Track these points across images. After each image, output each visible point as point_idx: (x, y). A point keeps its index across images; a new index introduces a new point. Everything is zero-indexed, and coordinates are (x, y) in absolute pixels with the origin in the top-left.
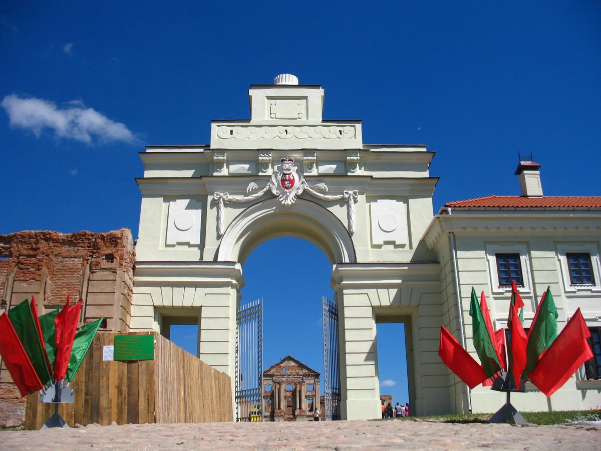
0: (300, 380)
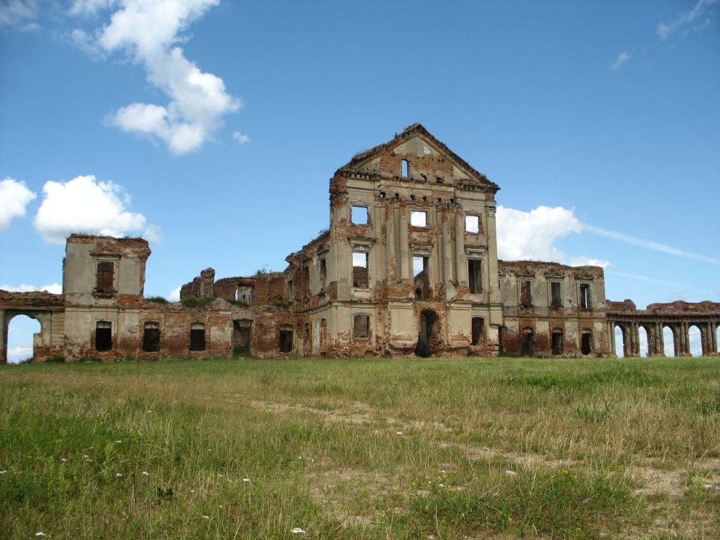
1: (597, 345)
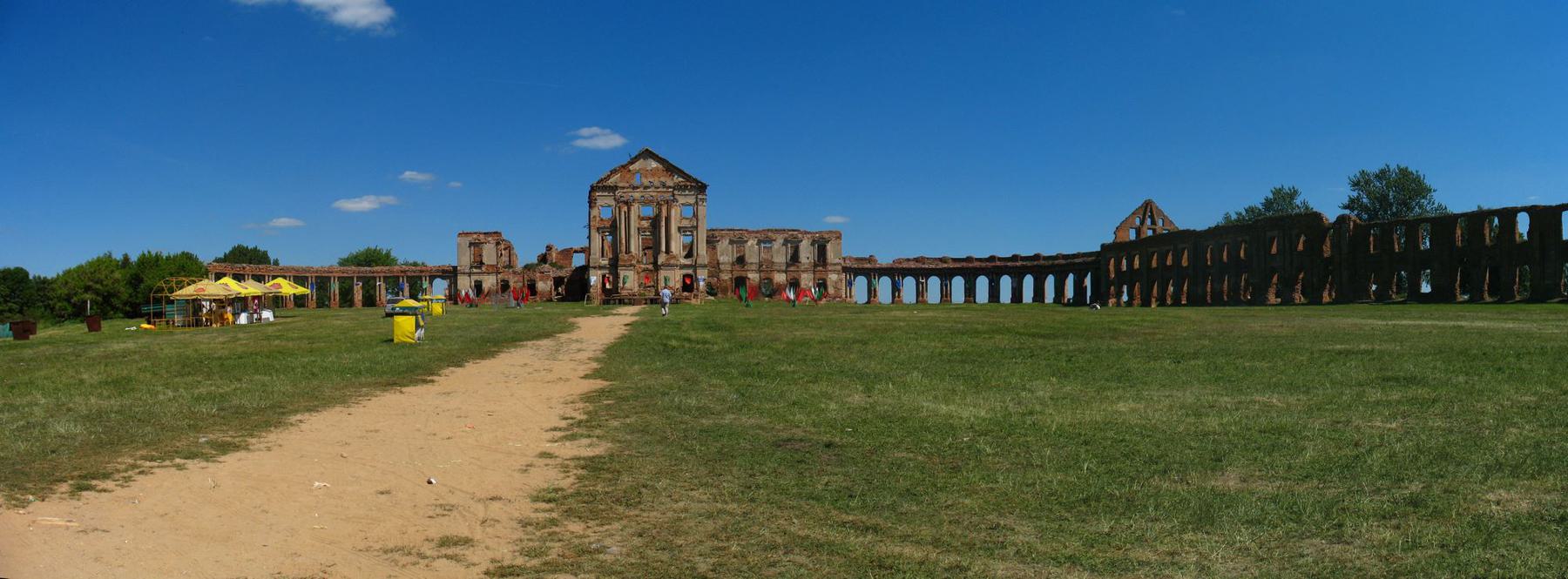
0: (668, 196)
1: (831, 290)
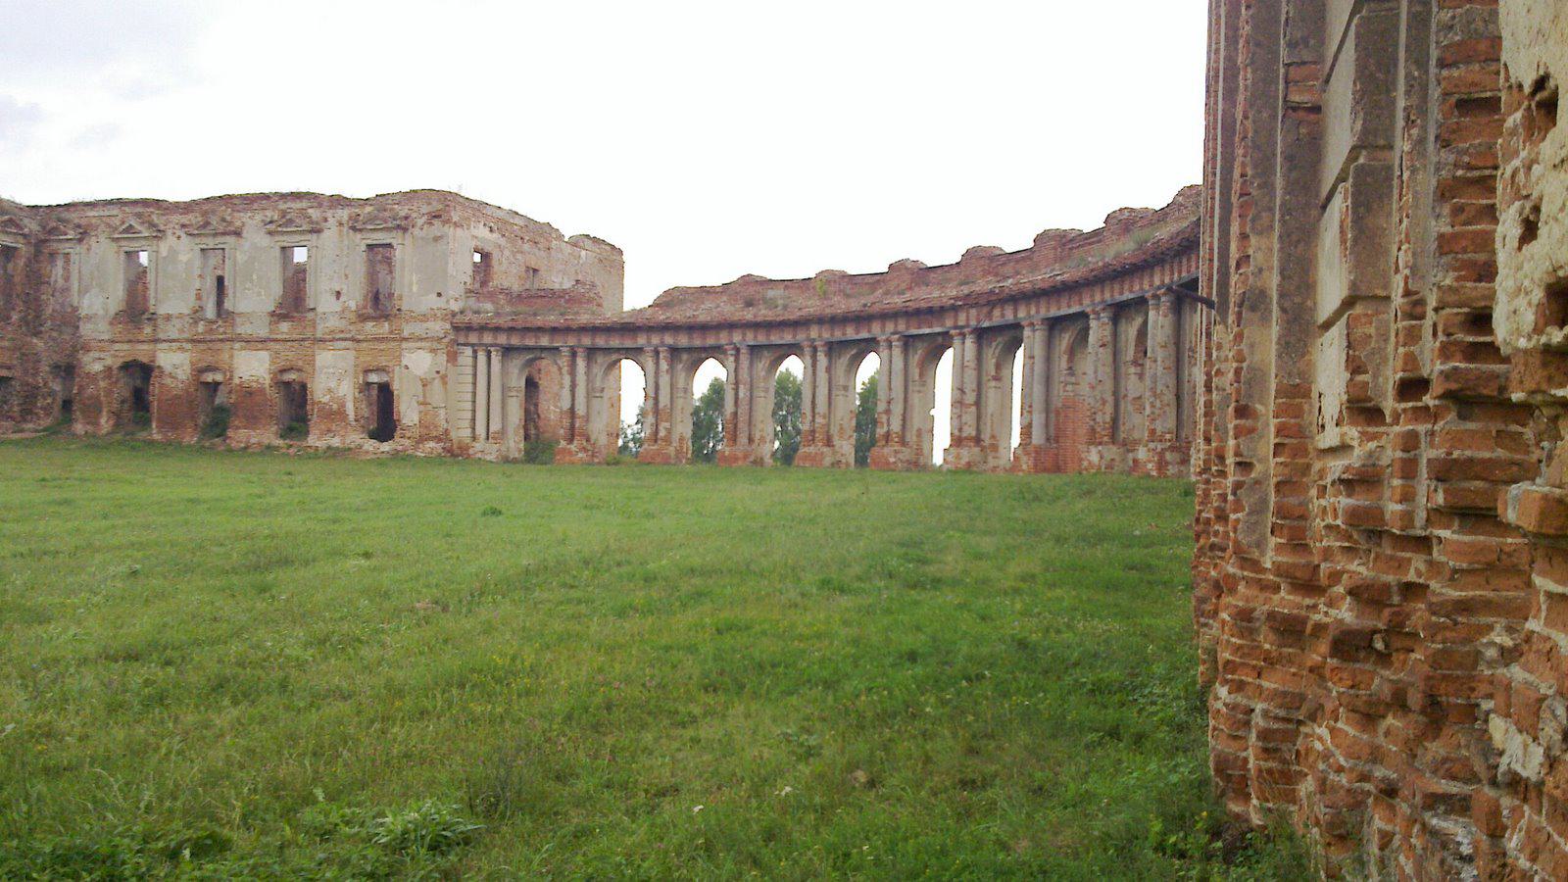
1: (408, 412)
